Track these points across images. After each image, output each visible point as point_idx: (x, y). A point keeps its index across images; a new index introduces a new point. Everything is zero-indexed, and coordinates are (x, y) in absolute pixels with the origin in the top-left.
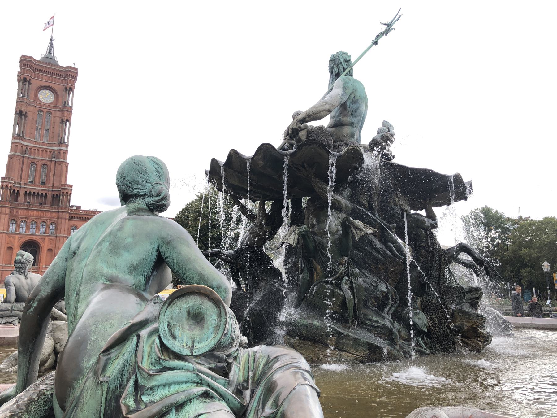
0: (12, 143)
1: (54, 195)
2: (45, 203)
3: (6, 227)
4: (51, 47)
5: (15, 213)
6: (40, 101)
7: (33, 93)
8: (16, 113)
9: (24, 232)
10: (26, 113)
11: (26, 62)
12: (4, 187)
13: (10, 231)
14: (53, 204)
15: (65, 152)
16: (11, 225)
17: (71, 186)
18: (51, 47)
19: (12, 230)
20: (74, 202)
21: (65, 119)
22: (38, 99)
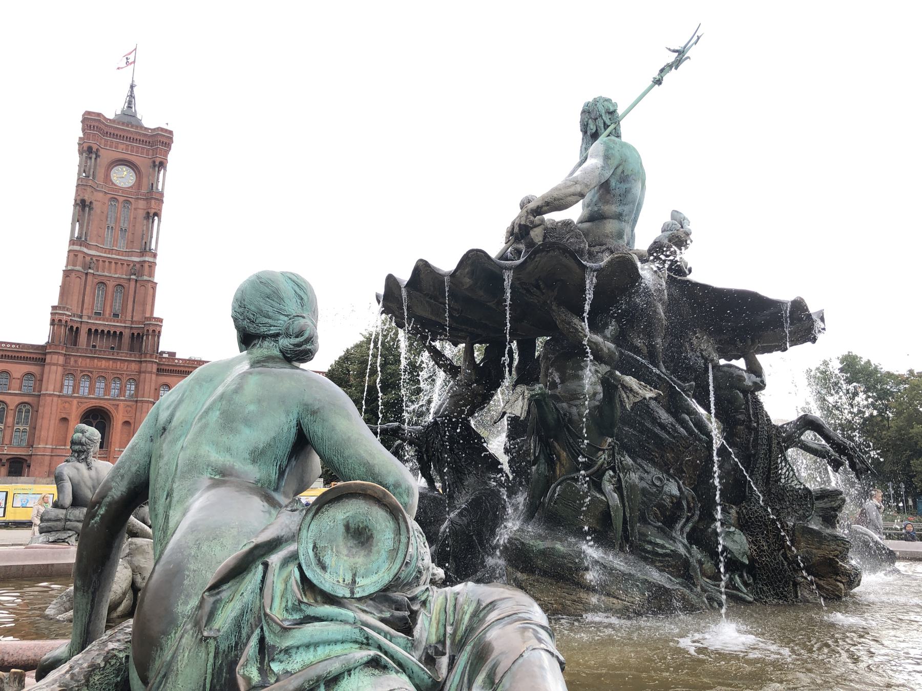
0: (69, 251)
1: (133, 334)
2: (120, 348)
3: (58, 386)
4: (131, 96)
5: (72, 363)
6: (113, 183)
8: (76, 204)
10: (91, 203)
11: (92, 123)
12: (56, 321)
13: (65, 392)
14: (132, 349)
15: (152, 265)
16: (66, 383)
17: (161, 320)
18: (131, 96)
19: (67, 390)
20: (165, 345)
21: (152, 211)
22: (111, 180)
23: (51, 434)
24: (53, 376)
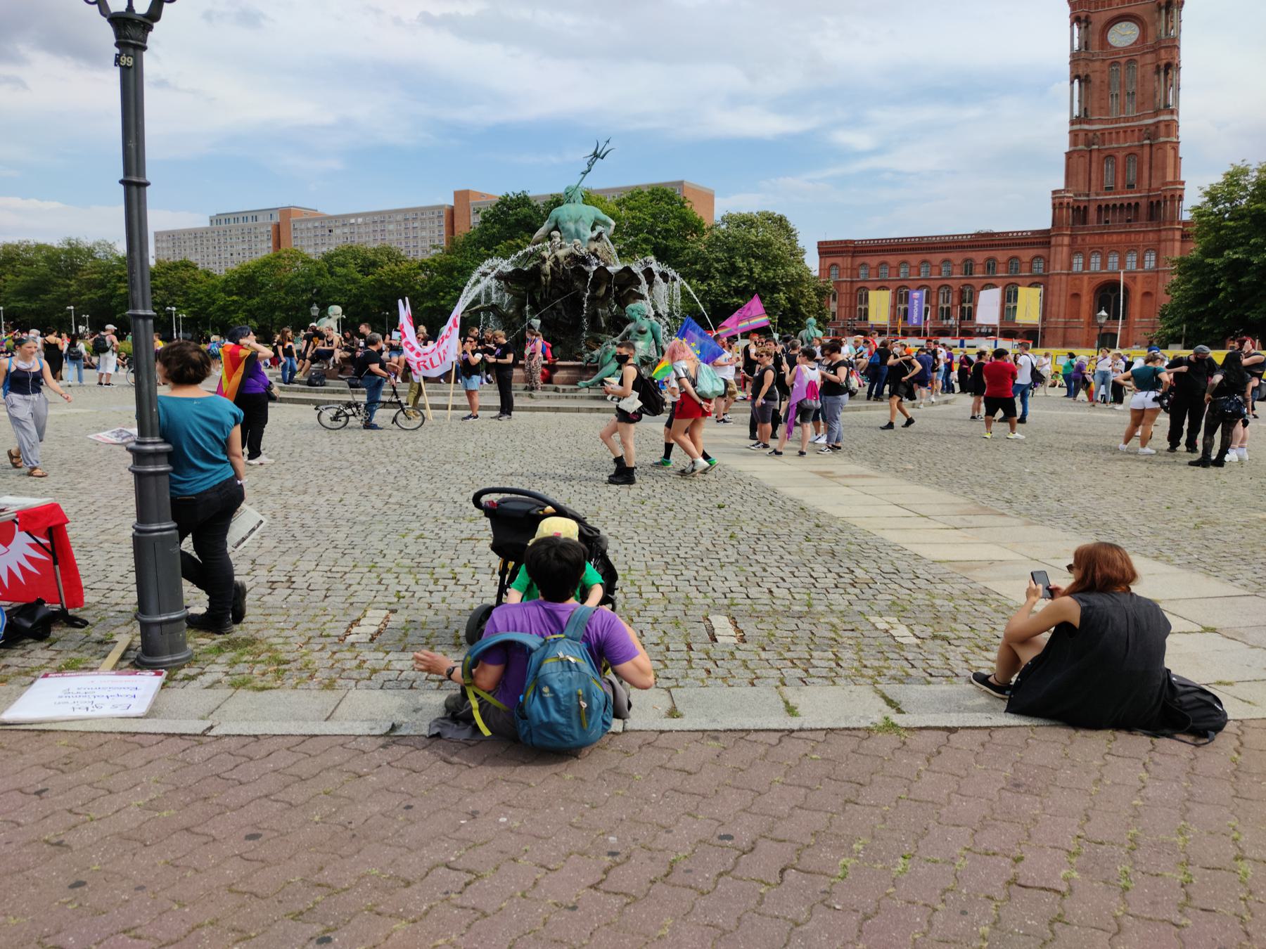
3: (1066, 264)
7: (1097, 37)
9: (1098, 269)
13: (1075, 269)
15: (1171, 127)
16: (1075, 261)
23: (1062, 309)
24: (1059, 257)
